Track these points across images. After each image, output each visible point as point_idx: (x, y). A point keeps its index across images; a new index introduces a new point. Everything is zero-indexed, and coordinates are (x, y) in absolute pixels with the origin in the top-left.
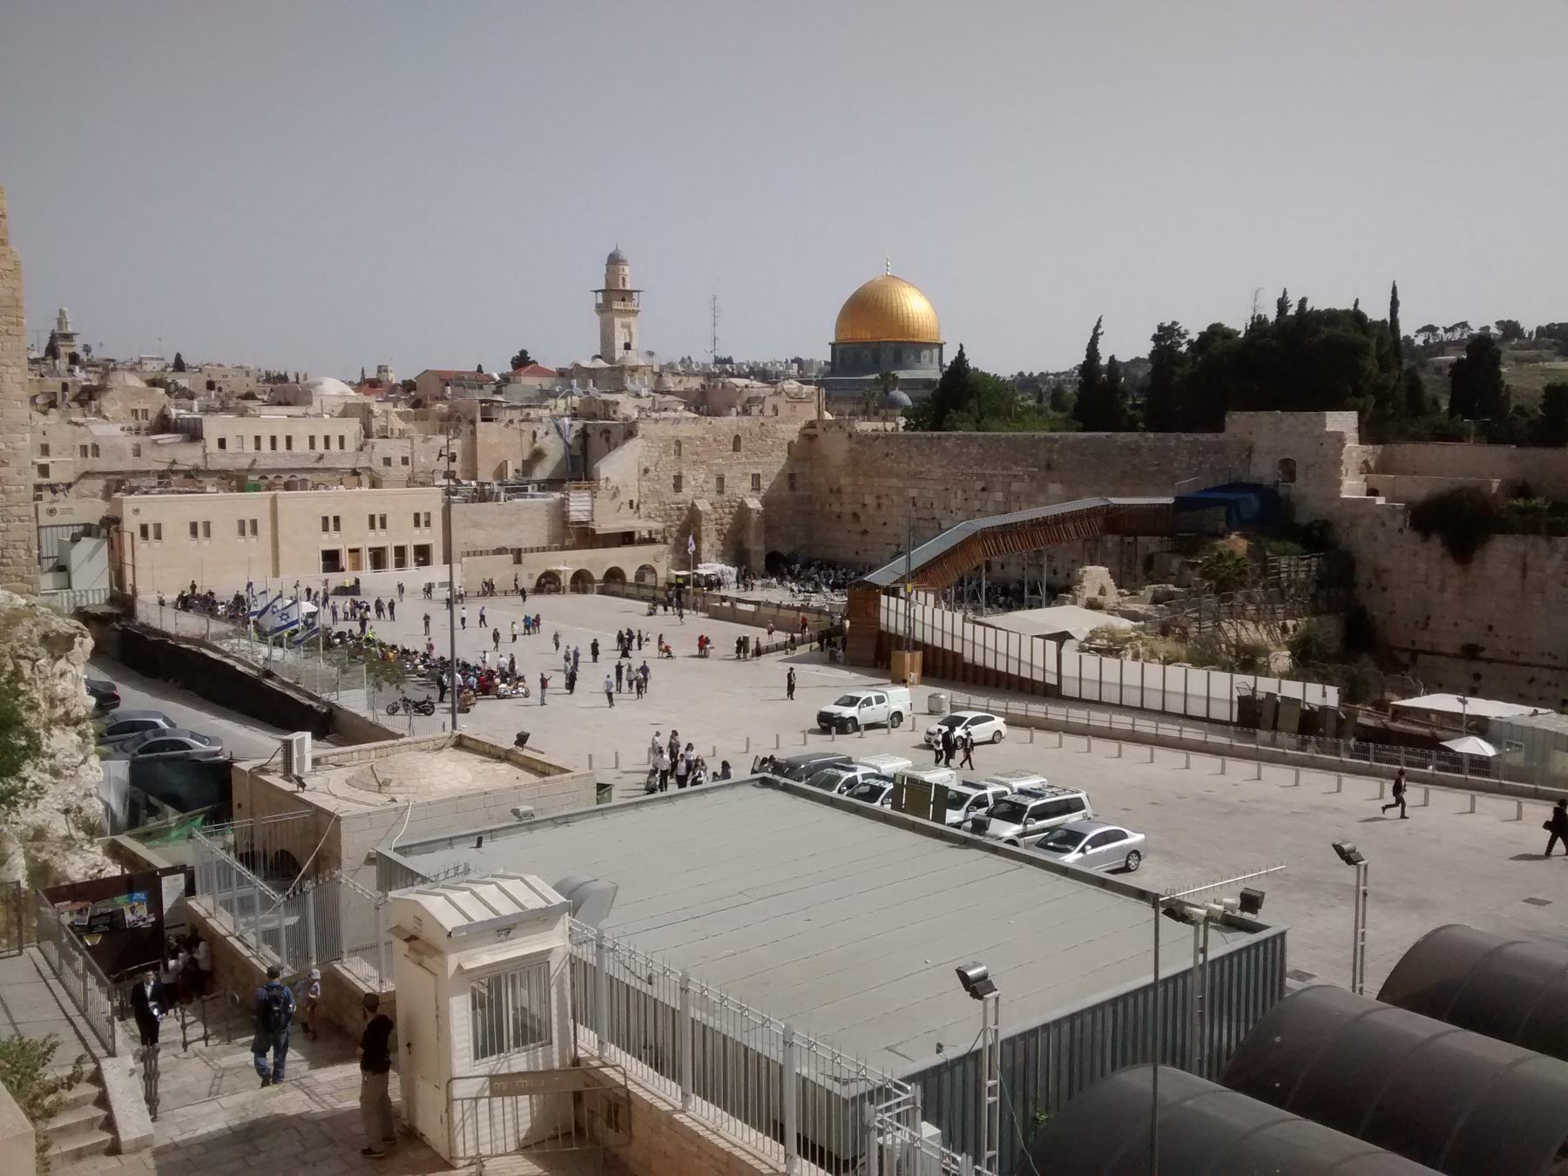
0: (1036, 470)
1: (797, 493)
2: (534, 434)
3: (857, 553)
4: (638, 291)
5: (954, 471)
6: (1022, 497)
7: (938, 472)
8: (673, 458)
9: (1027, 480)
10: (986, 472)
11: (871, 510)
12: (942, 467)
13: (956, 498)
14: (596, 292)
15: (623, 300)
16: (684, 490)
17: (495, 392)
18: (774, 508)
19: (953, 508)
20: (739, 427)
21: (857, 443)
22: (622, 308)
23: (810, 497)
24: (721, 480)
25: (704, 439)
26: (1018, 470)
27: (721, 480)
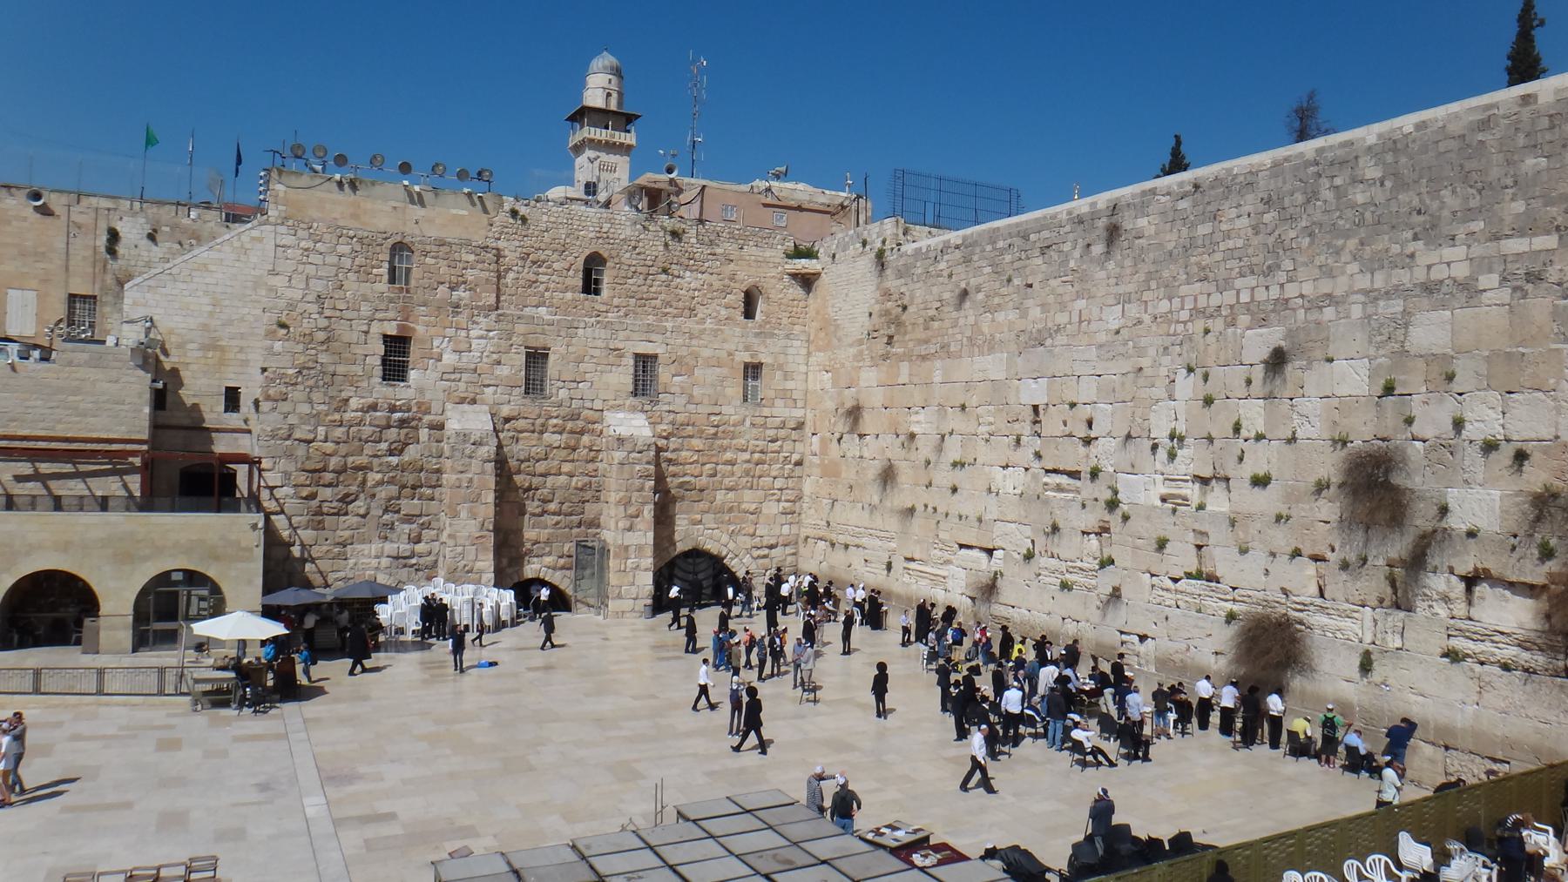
0: (1551, 241)
1: (766, 412)
2: (114, 236)
3: (889, 567)
5: (1164, 306)
6: (1466, 373)
7: (1113, 317)
8: (383, 286)
9: (1505, 295)
10: (1291, 290)
11: (925, 449)
12: (1123, 300)
13: (1171, 398)
16: (413, 375)
18: (697, 443)
19: (1162, 434)
21: (900, 275)
23: (800, 426)
24: (536, 358)
26: (1452, 261)
27: (536, 358)
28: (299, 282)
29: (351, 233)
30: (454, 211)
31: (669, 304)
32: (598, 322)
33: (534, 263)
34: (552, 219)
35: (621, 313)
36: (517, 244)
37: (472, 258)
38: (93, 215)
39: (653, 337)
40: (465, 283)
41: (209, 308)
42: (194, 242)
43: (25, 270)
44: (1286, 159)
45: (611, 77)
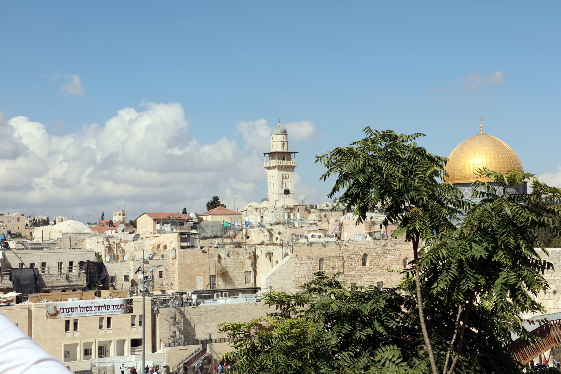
2: (219, 257)
4: (295, 153)
10: (556, 278)
14: (265, 154)
15: (284, 159)
17: (192, 228)
20: (366, 248)
22: (284, 165)
25: (340, 256)
28: (300, 273)
29: (310, 257)
30: (332, 247)
31: (384, 266)
32: (368, 274)
33: (351, 259)
34: (354, 245)
35: (372, 270)
36: (346, 254)
37: (337, 260)
38: (214, 251)
39: (381, 276)
40: (336, 267)
41: (282, 282)
42: (238, 255)
43: (200, 270)
44: (554, 251)
45: (284, 136)
